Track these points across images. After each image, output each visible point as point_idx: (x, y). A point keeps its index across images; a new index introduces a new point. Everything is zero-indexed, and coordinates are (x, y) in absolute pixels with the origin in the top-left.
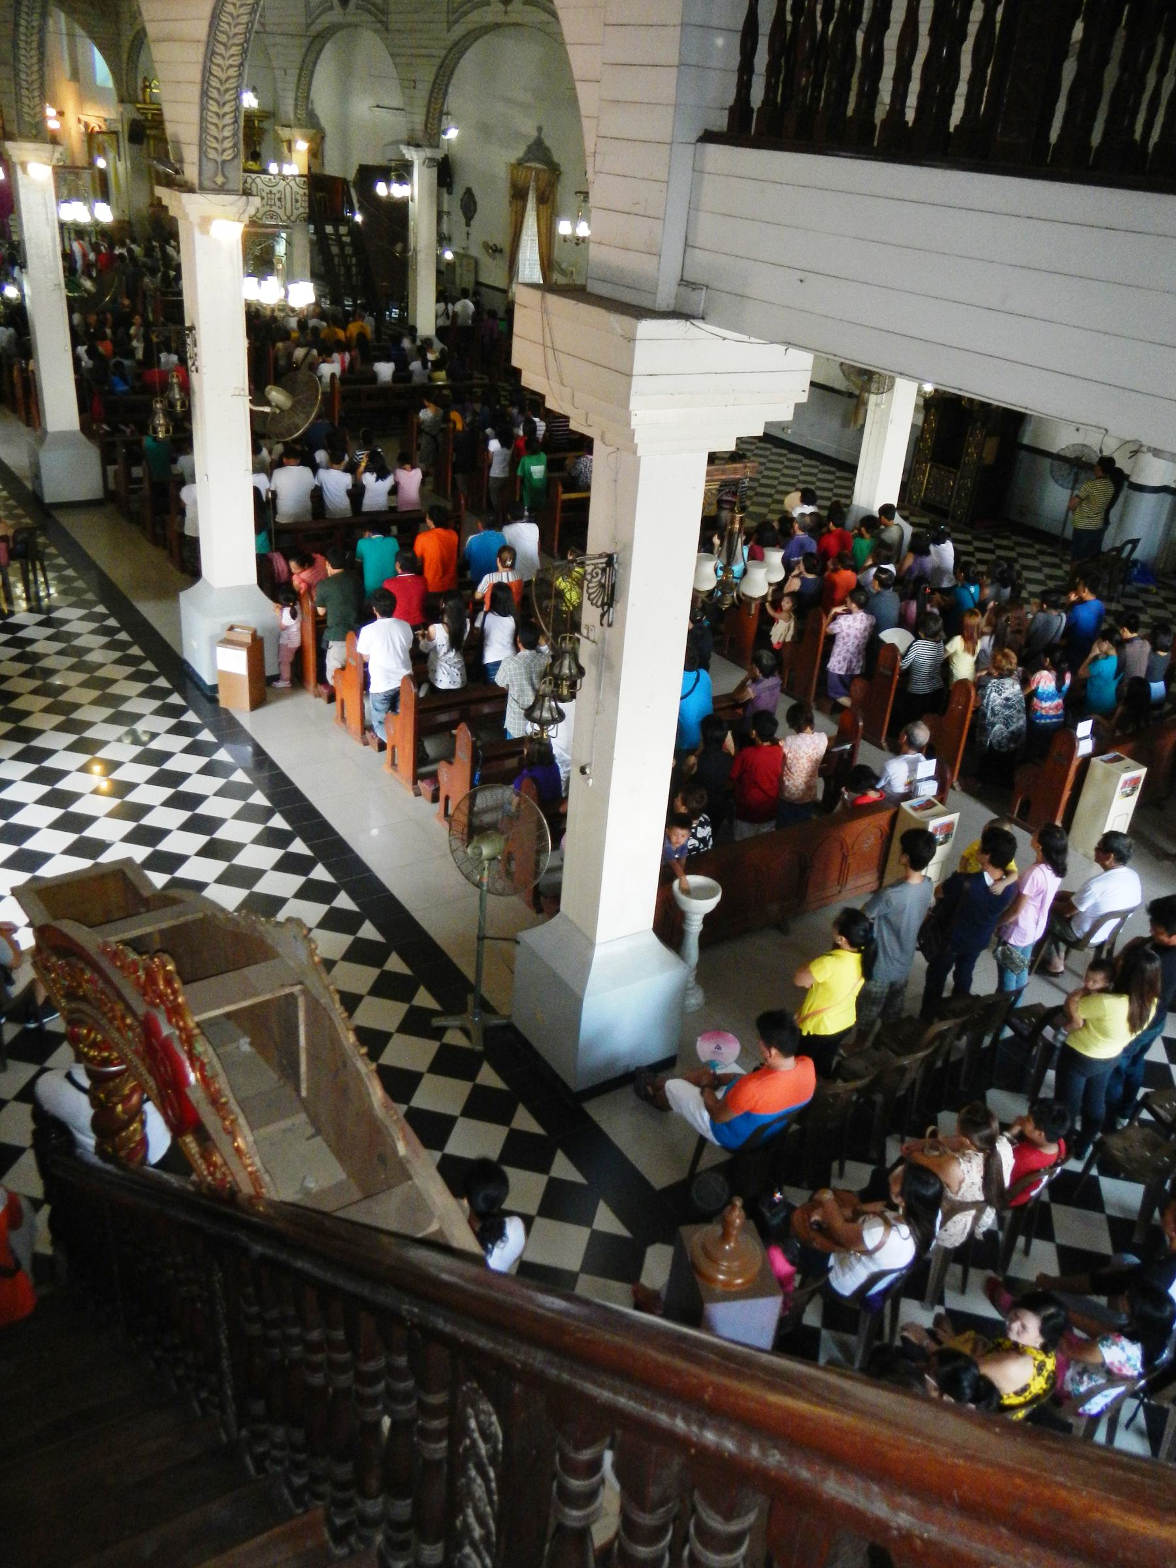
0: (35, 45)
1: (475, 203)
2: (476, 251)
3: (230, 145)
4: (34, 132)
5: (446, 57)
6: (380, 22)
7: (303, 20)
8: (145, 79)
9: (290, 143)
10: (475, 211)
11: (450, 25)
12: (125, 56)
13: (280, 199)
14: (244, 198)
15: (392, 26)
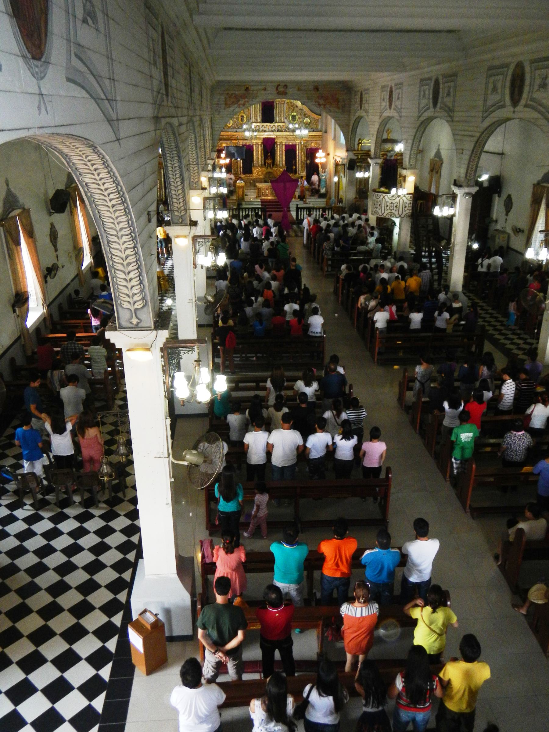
0: (178, 176)
1: (512, 203)
2: (509, 230)
3: (140, 297)
4: (180, 220)
5: (480, 136)
6: (450, 116)
7: (416, 115)
8: (360, 139)
9: (405, 177)
10: (511, 208)
11: (484, 118)
12: (351, 130)
13: (396, 206)
14: (155, 332)
15: (455, 119)
